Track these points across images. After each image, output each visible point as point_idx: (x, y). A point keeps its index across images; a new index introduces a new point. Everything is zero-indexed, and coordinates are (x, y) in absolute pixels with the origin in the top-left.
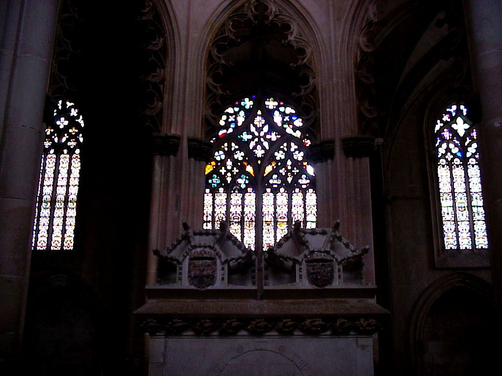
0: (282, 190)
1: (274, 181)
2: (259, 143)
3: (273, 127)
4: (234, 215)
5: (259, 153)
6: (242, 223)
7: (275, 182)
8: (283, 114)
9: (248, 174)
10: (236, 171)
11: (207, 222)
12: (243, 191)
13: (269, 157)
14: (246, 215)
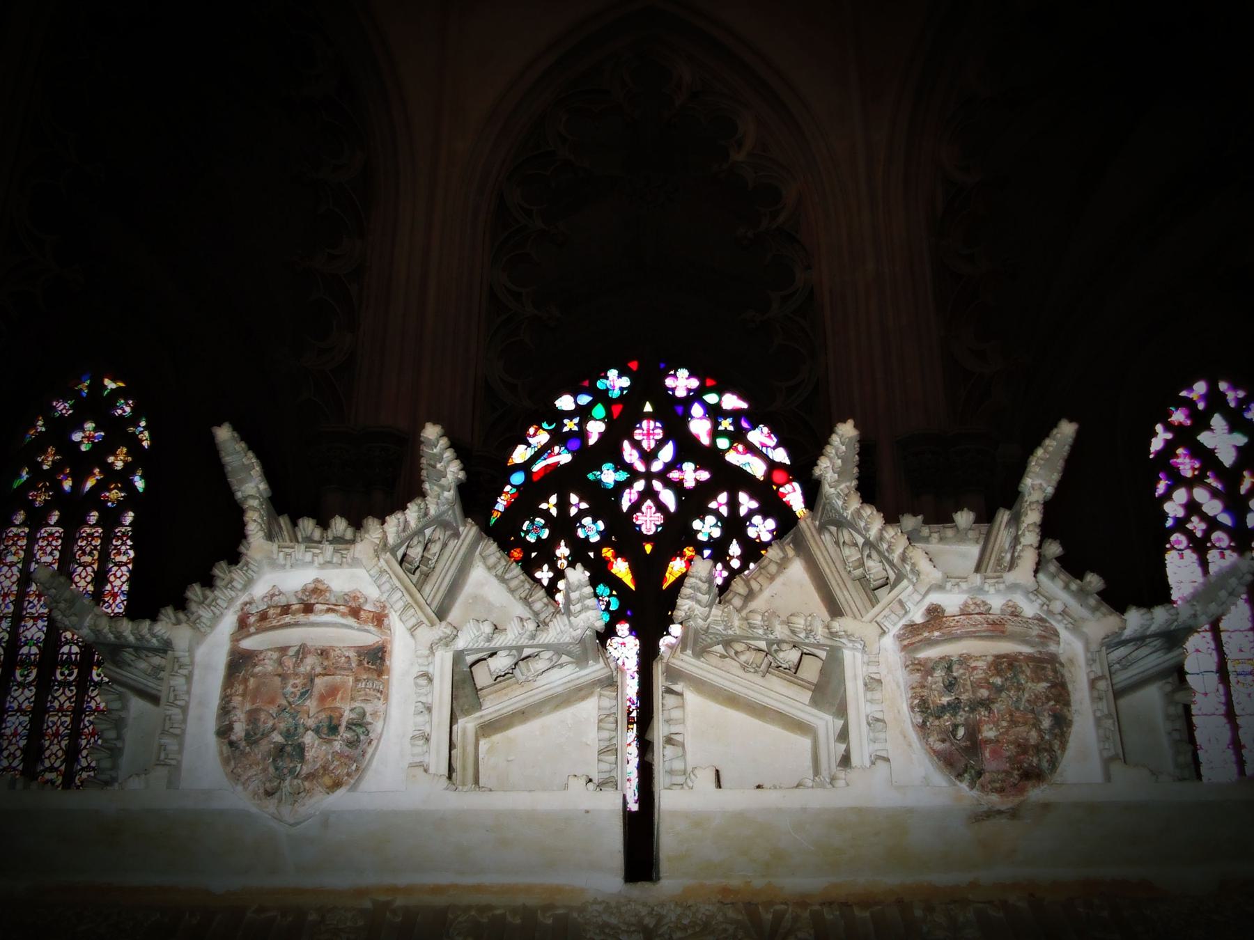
2: (649, 493)
3: (688, 449)
5: (649, 521)
8: (715, 413)
13: (677, 534)
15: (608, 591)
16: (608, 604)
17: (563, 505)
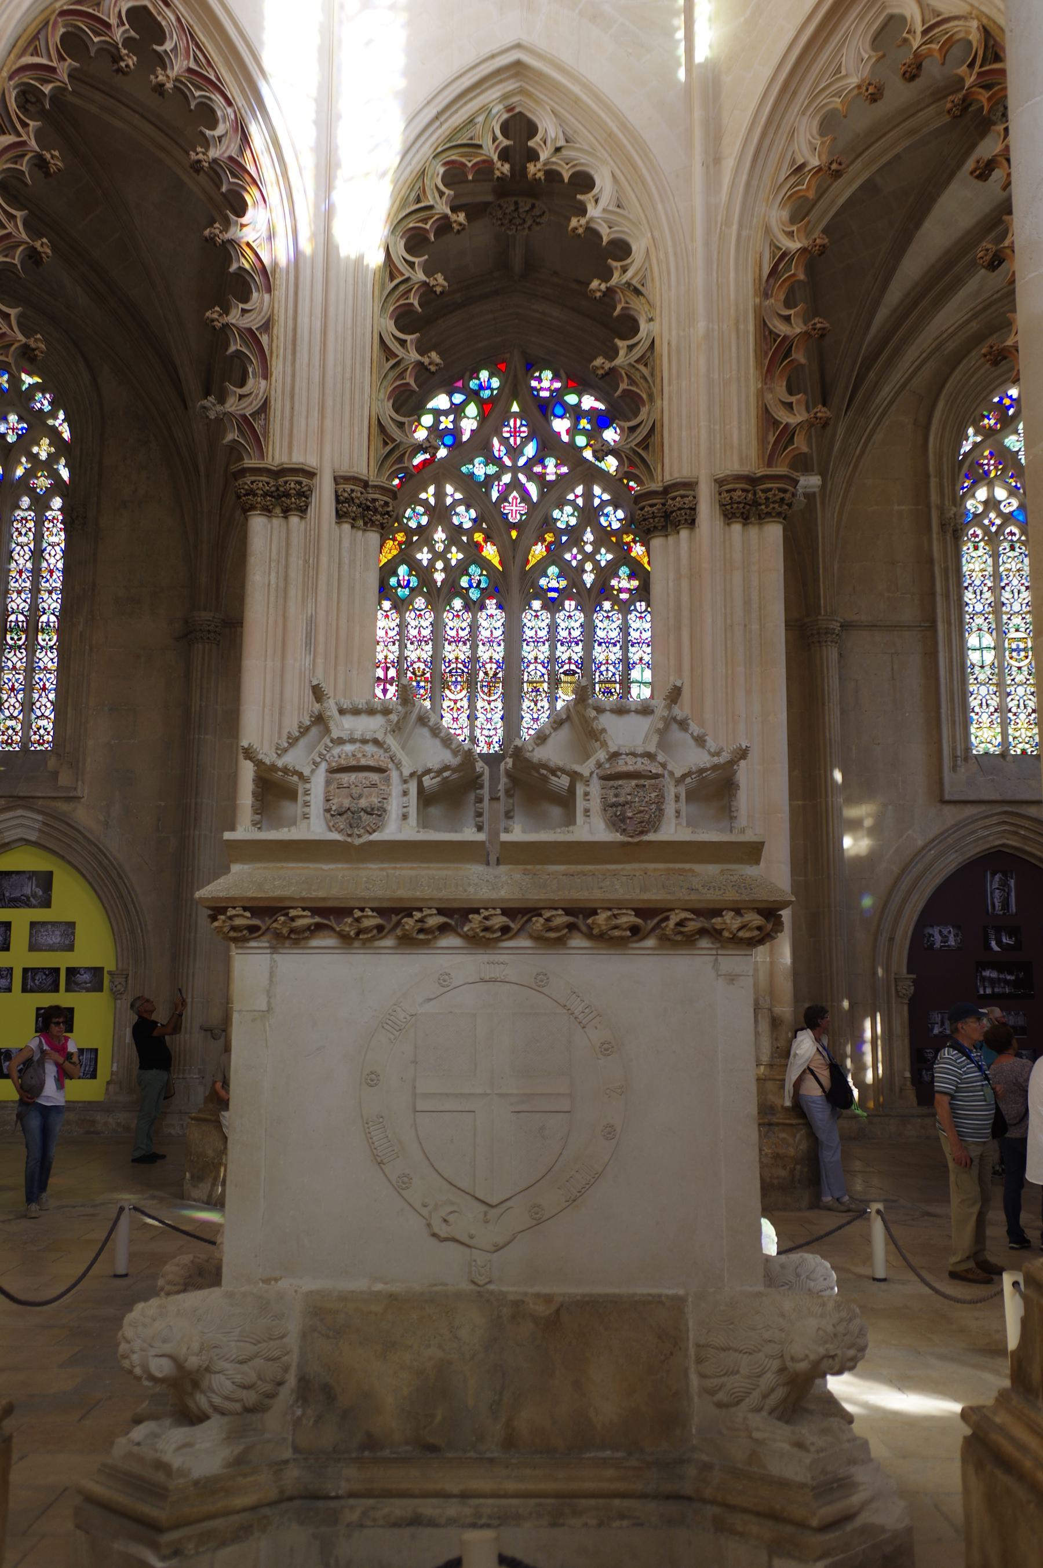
0: (570, 605)
1: (552, 579)
3: (549, 444)
4: (453, 666)
6: (471, 684)
7: (554, 584)
9: (485, 564)
10: (455, 556)
11: (385, 681)
12: (473, 607)
13: (540, 522)
14: (483, 665)
15: (479, 571)
16: (479, 582)
17: (440, 495)
